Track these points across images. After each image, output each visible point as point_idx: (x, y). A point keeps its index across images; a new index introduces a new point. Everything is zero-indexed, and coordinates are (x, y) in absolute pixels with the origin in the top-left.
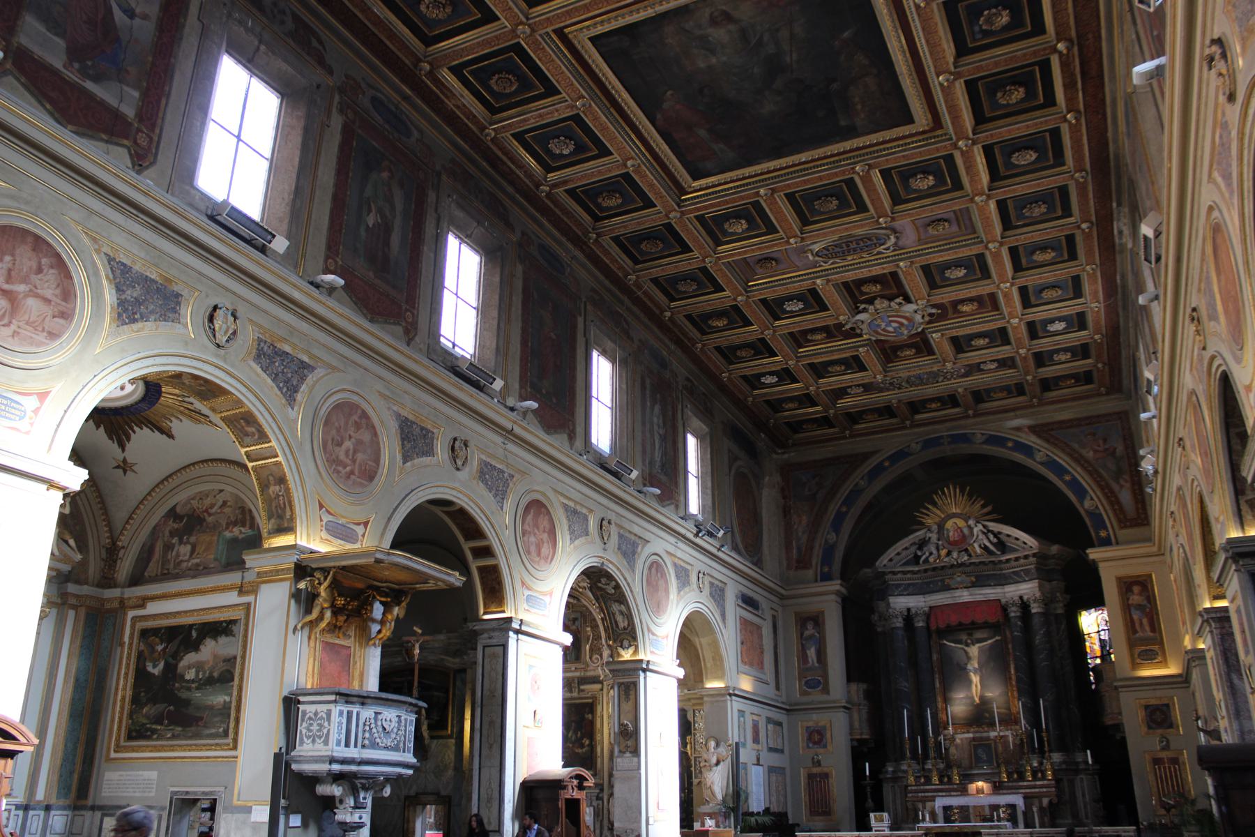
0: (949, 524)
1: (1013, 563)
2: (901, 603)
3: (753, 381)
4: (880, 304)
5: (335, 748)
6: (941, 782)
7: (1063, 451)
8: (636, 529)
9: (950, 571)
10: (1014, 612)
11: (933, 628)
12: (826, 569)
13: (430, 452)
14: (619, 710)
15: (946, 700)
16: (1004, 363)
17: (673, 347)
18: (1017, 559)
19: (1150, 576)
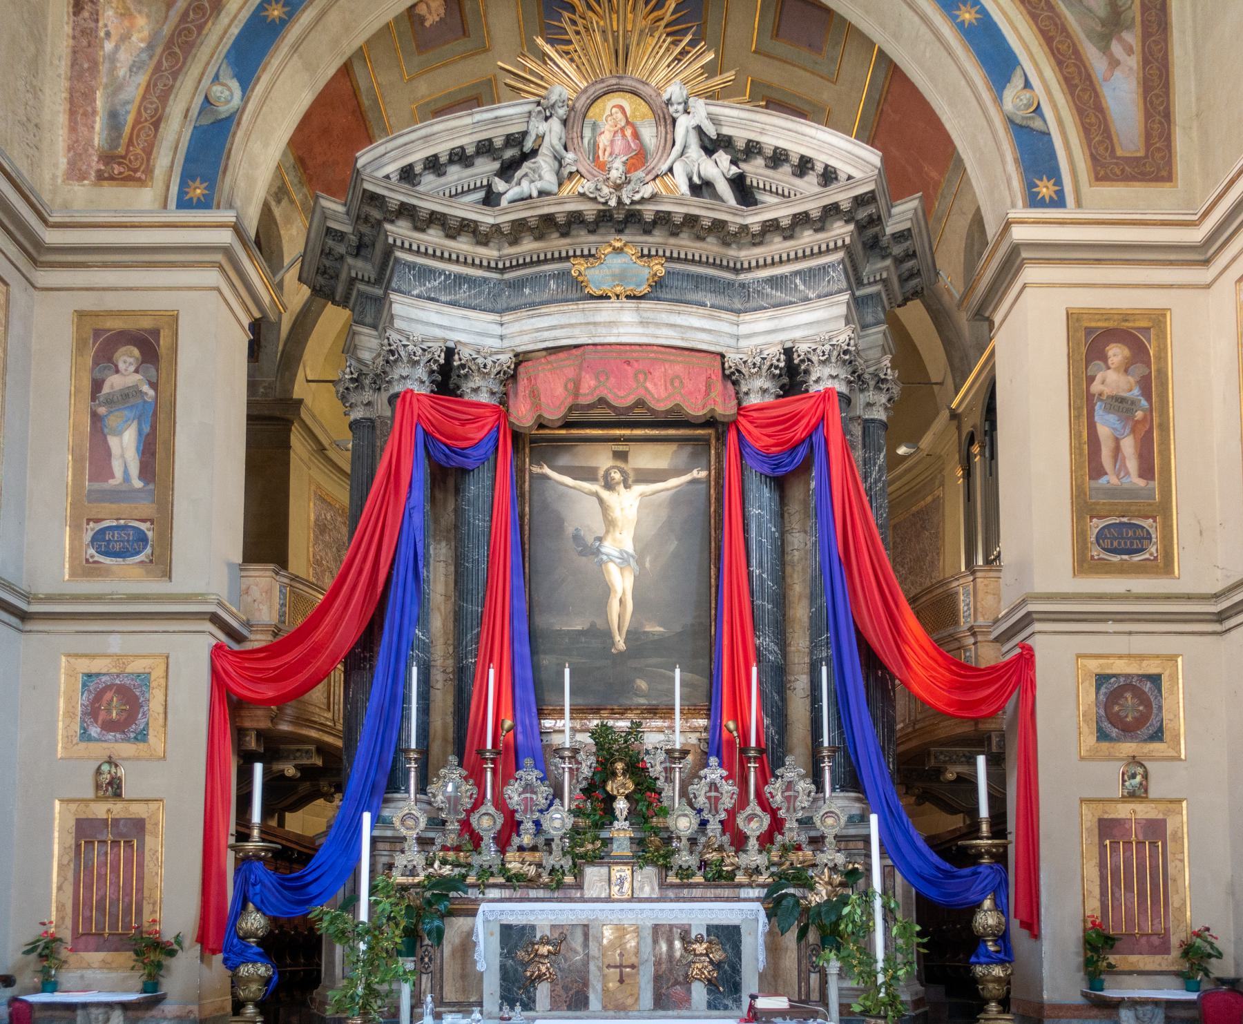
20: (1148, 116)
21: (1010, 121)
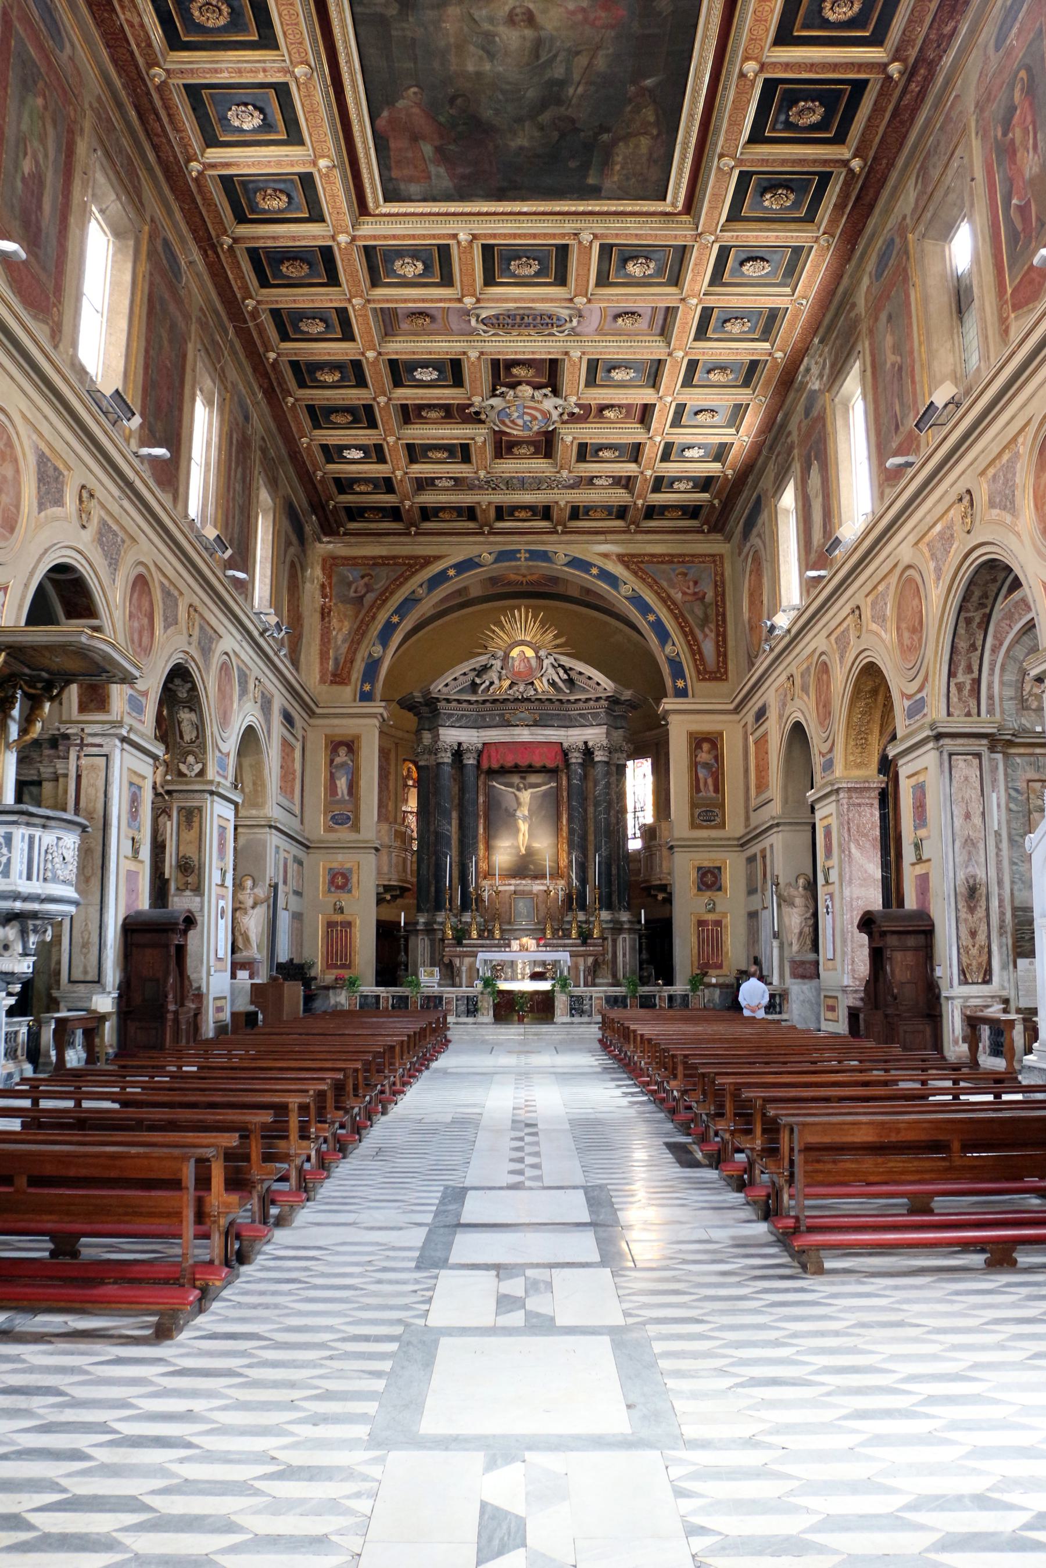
0: (515, 653)
1: (581, 704)
2: (451, 736)
3: (332, 453)
4: (526, 391)
5: (19, 882)
6: (480, 937)
7: (651, 587)
8: (214, 622)
9: (511, 705)
10: (576, 758)
11: (485, 766)
12: (367, 687)
13: (59, 502)
14: (178, 840)
15: (488, 848)
16: (627, 483)
17: (260, 396)
18: (587, 700)
19: (721, 734)
20: (718, 656)
21: (667, 658)
